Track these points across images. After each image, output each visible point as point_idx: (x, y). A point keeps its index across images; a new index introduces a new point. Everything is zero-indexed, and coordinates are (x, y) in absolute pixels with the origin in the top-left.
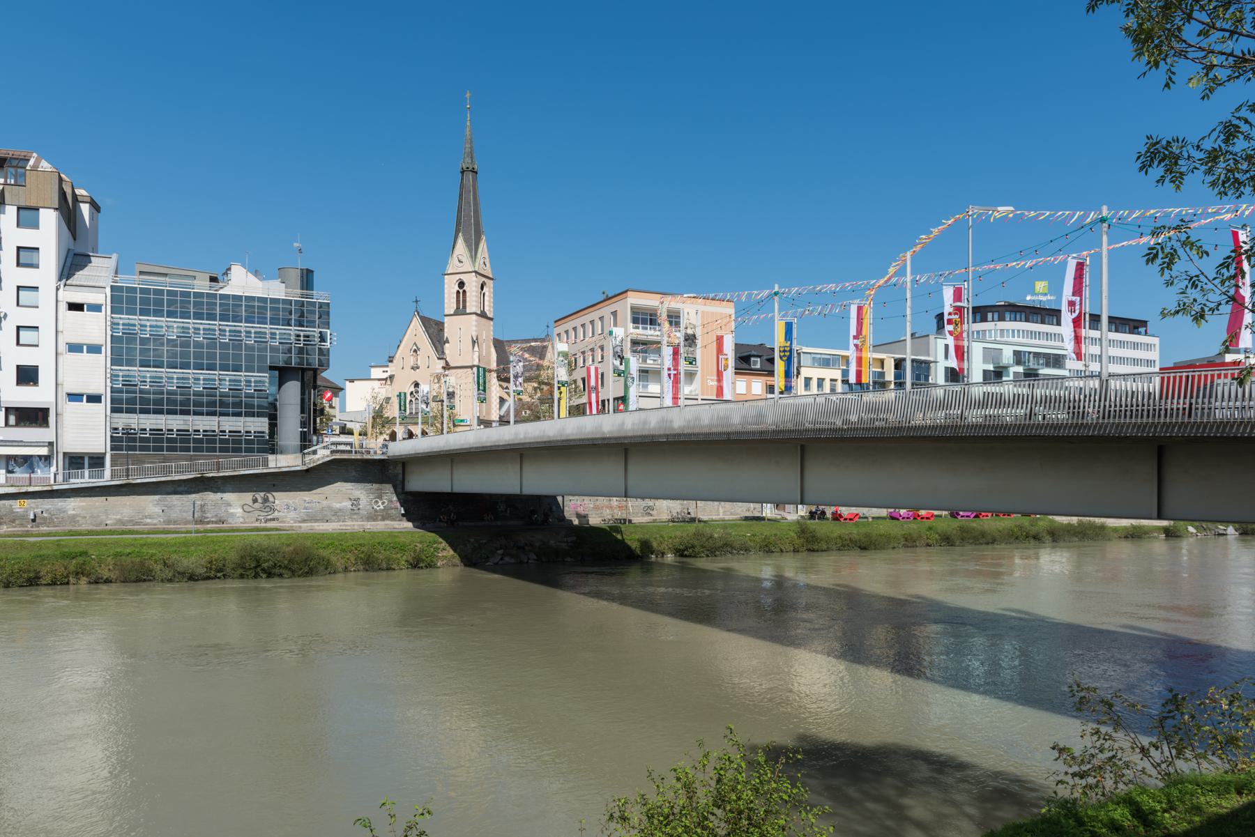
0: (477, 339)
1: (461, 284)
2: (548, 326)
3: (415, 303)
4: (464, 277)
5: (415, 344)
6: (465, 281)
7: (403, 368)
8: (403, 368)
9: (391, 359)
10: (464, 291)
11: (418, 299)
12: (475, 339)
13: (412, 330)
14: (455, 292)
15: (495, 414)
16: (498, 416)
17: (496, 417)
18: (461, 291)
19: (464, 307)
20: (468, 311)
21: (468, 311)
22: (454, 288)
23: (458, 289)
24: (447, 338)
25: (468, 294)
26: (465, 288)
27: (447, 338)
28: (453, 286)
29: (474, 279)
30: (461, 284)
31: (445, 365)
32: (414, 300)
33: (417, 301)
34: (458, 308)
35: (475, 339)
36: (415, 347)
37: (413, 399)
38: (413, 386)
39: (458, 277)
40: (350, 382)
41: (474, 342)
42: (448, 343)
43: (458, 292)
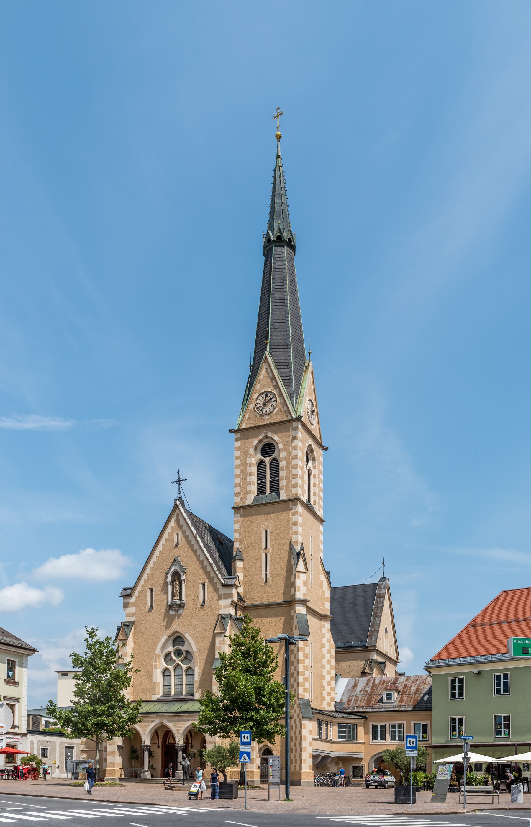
3: (176, 485)
9: (129, 592)
13: (170, 535)
15: (328, 699)
16: (333, 703)
17: (329, 704)
18: (267, 460)
19: (275, 488)
21: (283, 496)
23: (259, 456)
32: (175, 478)
33: (179, 481)
34: (261, 490)
37: (171, 668)
38: (170, 643)
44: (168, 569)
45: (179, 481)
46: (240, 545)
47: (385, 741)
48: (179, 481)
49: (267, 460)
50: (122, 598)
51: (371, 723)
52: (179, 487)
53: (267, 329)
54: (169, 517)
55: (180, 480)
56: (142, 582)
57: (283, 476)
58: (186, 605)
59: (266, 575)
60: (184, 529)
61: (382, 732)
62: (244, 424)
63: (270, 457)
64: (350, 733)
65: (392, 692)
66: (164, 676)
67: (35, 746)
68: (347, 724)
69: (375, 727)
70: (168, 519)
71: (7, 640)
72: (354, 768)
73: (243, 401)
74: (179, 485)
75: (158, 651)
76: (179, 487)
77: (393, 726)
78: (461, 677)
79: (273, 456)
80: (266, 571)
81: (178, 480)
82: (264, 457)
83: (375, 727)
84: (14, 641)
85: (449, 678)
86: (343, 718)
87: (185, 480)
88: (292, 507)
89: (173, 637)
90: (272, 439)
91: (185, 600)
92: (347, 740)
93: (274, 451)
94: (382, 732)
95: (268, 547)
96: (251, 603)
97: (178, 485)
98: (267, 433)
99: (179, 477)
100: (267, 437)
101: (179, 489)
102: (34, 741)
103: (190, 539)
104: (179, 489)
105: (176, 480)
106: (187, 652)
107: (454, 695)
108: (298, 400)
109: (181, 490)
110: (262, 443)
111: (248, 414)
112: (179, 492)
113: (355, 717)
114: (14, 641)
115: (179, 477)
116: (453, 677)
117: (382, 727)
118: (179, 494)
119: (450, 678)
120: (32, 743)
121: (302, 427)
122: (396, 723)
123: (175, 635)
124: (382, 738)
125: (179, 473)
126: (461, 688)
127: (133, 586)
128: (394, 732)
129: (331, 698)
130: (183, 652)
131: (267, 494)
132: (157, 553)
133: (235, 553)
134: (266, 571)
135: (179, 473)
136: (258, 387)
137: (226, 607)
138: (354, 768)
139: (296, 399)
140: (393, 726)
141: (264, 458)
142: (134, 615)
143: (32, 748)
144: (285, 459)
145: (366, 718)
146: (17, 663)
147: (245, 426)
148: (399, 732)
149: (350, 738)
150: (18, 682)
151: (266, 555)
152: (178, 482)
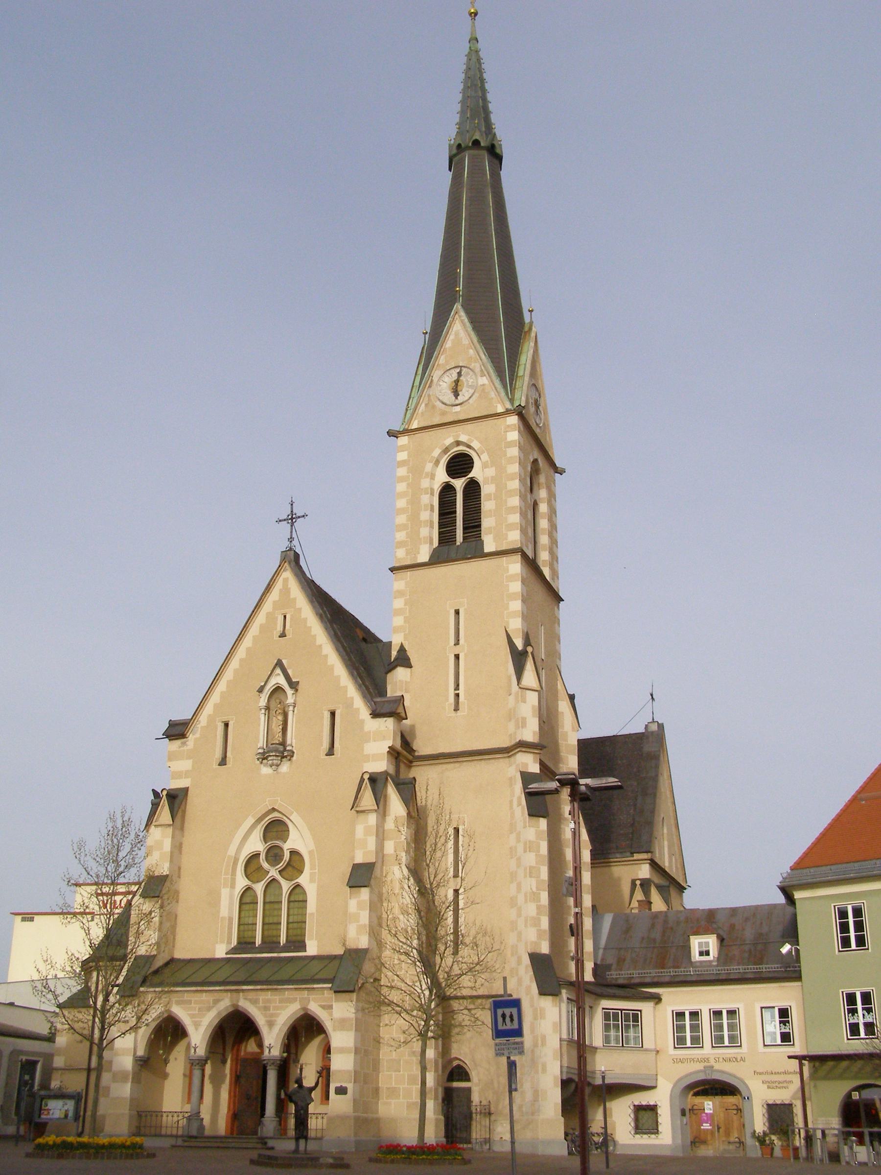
0: (527, 642)
3: (286, 526)
5: (279, 664)
7: (223, 762)
8: (223, 762)
10: (473, 490)
11: (298, 511)
12: (519, 644)
13: (270, 616)
14: (437, 487)
18: (459, 484)
20: (489, 546)
22: (432, 476)
24: (402, 650)
25: (486, 490)
26: (476, 473)
27: (402, 650)
28: (429, 467)
29: (514, 436)
31: (398, 745)
32: (285, 513)
33: (292, 519)
35: (519, 644)
36: (280, 680)
38: (258, 832)
39: (447, 438)
40: (23, 920)
41: (519, 658)
42: (409, 666)
43: (447, 490)
44: (263, 684)
45: (292, 519)
46: (405, 638)
47: (702, 1047)
48: (292, 519)
49: (459, 484)
52: (292, 529)
53: (458, 270)
54: (269, 584)
55: (294, 516)
56: (208, 709)
57: (490, 511)
58: (295, 755)
59: (457, 695)
60: (297, 607)
61: (695, 1028)
62: (416, 422)
63: (464, 479)
66: (241, 903)
68: (621, 1010)
70: (266, 589)
72: (639, 1109)
73: (413, 387)
74: (292, 526)
75: (232, 851)
76: (292, 529)
78: (857, 902)
79: (470, 476)
80: (457, 687)
81: (290, 517)
82: (453, 478)
83: (680, 1015)
85: (833, 905)
88: (508, 567)
89: (263, 822)
90: (469, 447)
91: (294, 745)
93: (472, 467)
94: (695, 1028)
95: (462, 641)
96: (421, 753)
97: (289, 525)
98: (458, 436)
99: (292, 511)
100: (458, 443)
101: (291, 532)
103: (309, 625)
104: (291, 532)
105: (285, 517)
106: (294, 853)
107: (846, 942)
108: (514, 382)
109: (294, 535)
110: (449, 454)
111: (423, 405)
112: (291, 538)
115: (292, 511)
116: (840, 904)
117: (695, 1015)
118: (291, 542)
119: (835, 906)
121: (524, 428)
123: (270, 816)
124: (697, 1041)
125: (292, 505)
126: (859, 926)
127: (190, 718)
128: (720, 1027)
130: (285, 851)
131: (458, 543)
132: (241, 652)
133: (394, 653)
134: (457, 687)
135: (292, 505)
136: (442, 360)
137: (376, 757)
138: (639, 1109)
139: (511, 380)
140: (718, 1014)
141: (452, 480)
142: (187, 774)
144: (493, 479)
147: (418, 424)
148: (731, 1027)
151: (457, 657)
152: (290, 521)
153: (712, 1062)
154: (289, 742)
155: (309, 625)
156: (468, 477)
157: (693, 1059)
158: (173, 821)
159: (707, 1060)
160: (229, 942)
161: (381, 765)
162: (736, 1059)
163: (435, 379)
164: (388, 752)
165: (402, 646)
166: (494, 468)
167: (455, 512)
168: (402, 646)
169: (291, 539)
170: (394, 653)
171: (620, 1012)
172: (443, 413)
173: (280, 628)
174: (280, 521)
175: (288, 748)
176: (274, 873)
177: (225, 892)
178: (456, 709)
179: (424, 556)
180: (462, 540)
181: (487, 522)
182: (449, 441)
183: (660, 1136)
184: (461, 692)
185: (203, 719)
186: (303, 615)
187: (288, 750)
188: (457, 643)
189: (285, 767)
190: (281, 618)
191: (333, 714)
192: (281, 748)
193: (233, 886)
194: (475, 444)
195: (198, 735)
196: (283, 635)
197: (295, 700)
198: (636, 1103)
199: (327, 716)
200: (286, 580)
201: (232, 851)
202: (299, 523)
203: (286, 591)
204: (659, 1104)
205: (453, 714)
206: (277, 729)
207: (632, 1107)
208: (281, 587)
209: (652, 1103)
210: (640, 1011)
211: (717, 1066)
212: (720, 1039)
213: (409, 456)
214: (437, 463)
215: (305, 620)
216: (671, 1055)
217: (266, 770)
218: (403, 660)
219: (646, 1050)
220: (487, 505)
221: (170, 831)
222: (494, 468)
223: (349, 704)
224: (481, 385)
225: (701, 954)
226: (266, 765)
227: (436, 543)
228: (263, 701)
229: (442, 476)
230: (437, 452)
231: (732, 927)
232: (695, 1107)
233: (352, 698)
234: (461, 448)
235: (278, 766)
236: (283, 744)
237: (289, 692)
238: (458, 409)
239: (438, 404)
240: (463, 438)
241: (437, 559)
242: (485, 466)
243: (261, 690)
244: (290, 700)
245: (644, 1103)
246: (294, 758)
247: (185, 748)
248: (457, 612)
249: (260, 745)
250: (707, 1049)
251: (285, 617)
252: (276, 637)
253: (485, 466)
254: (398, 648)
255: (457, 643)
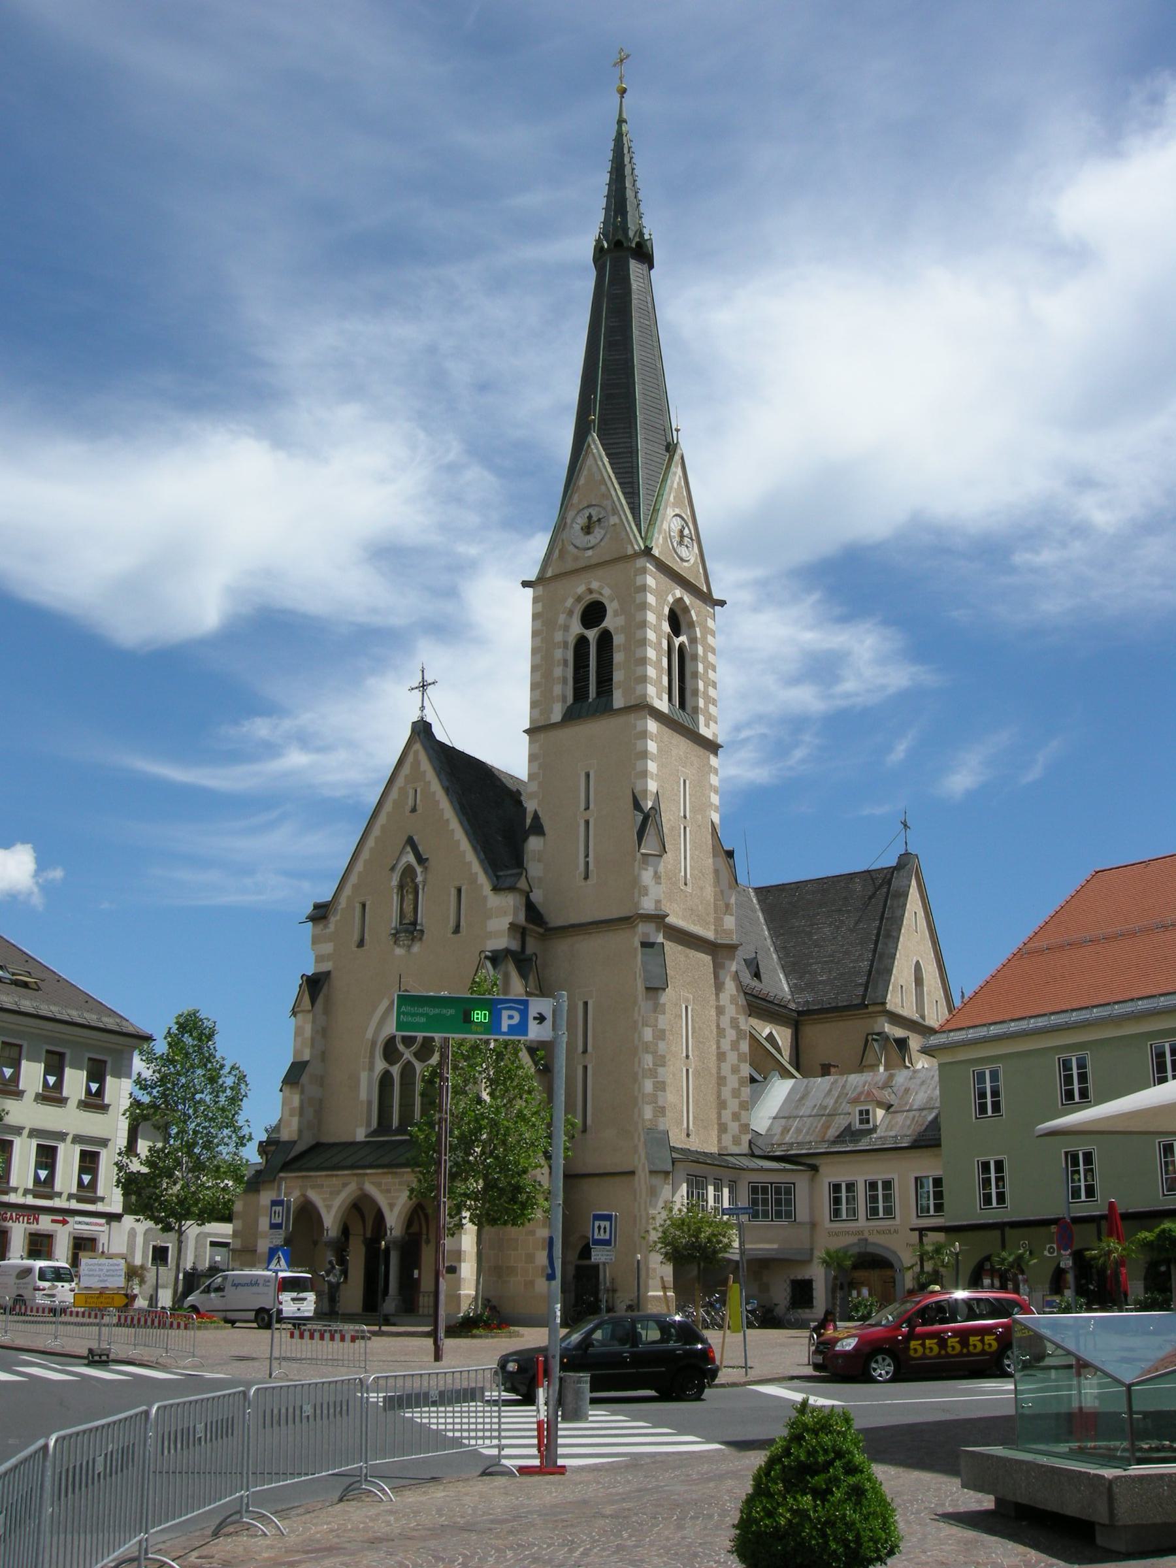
1: (593, 613)
2: (905, 825)
3: (417, 694)
4: (601, 587)
5: (411, 842)
6: (606, 595)
7: (361, 944)
8: (361, 944)
10: (606, 639)
11: (429, 678)
13: (402, 791)
14: (572, 640)
16: (746, 1138)
18: (592, 635)
22: (566, 628)
24: (536, 817)
25: (618, 640)
26: (609, 623)
28: (562, 619)
30: (593, 613)
31: (521, 919)
33: (423, 686)
34: (580, 692)
36: (410, 858)
43: (582, 642)
48: (423, 686)
49: (592, 635)
50: (310, 924)
51: (826, 1181)
56: (347, 891)
61: (851, 1200)
63: (596, 629)
64: (778, 1202)
65: (870, 1108)
67: (140, 1240)
68: (771, 1184)
69: (837, 1188)
71: (91, 1018)
77: (873, 1185)
79: (603, 625)
83: (837, 1188)
84: (105, 1019)
86: (762, 1170)
87: (434, 683)
92: (772, 1220)
97: (421, 693)
98: (590, 583)
99: (423, 678)
100: (590, 591)
101: (423, 700)
102: (137, 1231)
104: (423, 700)
105: (417, 685)
109: (427, 703)
112: (423, 706)
113: (788, 1166)
114: (105, 1019)
115: (423, 678)
117: (851, 1187)
120: (132, 1233)
122: (880, 1177)
125: (423, 671)
128: (874, 1199)
129: (741, 1125)
131: (590, 700)
133: (529, 821)
135: (423, 671)
140: (873, 1185)
143: (131, 1246)
145: (814, 1168)
146: (109, 1065)
149: (779, 1215)
150: (108, 1106)
153: (866, 1234)
154: (419, 922)
155: (437, 799)
156: (601, 626)
157: (848, 1232)
158: (312, 1006)
159: (861, 1232)
160: (369, 1124)
161: (502, 942)
162: (890, 1231)
163: (569, 521)
164: (509, 928)
165: (536, 812)
166: (623, 617)
167: (588, 666)
168: (536, 812)
169: (422, 708)
170: (529, 821)
171: (769, 1185)
172: (576, 559)
173: (410, 802)
174: (412, 689)
175: (418, 928)
176: (408, 1055)
177: (364, 1076)
178: (586, 877)
179: (557, 716)
180: (594, 696)
181: (618, 676)
182: (581, 589)
183: (814, 1310)
184: (591, 859)
185: (343, 901)
186: (432, 789)
187: (418, 930)
188: (587, 808)
189: (416, 948)
190: (411, 792)
191: (459, 891)
192: (411, 928)
193: (371, 1068)
194: (607, 591)
195: (338, 917)
196: (414, 810)
197: (425, 879)
198: (792, 1277)
199: (453, 892)
200: (416, 753)
201: (370, 1034)
202: (430, 689)
203: (416, 764)
204: (814, 1278)
205: (583, 883)
206: (408, 908)
207: (788, 1282)
208: (412, 760)
209: (807, 1278)
210: (794, 1184)
211: (871, 1239)
212: (874, 1211)
213: (543, 606)
214: (570, 613)
215: (434, 793)
216: (827, 1228)
217: (399, 951)
218: (538, 828)
219: (799, 1223)
220: (618, 657)
221: (310, 1016)
222: (623, 617)
223: (473, 880)
224: (613, 525)
225: (861, 1122)
226: (399, 946)
227: (570, 700)
228: (395, 882)
229: (576, 628)
230: (570, 602)
231: (907, 1090)
232: (854, 1281)
233: (476, 873)
234: (595, 596)
235: (409, 947)
236: (414, 923)
237: (419, 870)
238: (590, 553)
239: (571, 548)
240: (595, 585)
241: (571, 716)
242: (616, 614)
243: (393, 869)
244: (419, 879)
245: (799, 1277)
246: (425, 937)
247: (328, 931)
248: (588, 775)
249: (393, 925)
250: (862, 1222)
251: (416, 791)
252: (407, 813)
253: (616, 614)
254: (532, 816)
255: (587, 808)
